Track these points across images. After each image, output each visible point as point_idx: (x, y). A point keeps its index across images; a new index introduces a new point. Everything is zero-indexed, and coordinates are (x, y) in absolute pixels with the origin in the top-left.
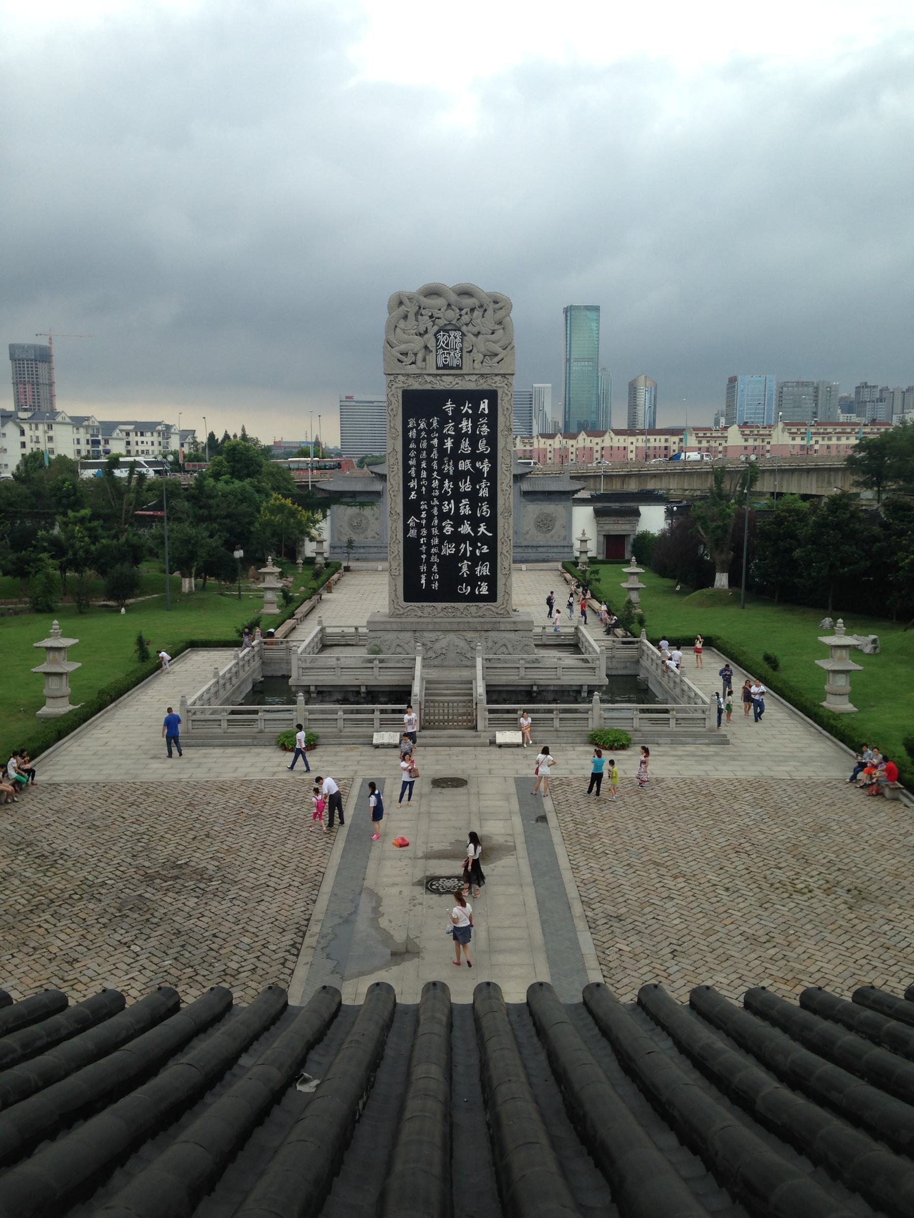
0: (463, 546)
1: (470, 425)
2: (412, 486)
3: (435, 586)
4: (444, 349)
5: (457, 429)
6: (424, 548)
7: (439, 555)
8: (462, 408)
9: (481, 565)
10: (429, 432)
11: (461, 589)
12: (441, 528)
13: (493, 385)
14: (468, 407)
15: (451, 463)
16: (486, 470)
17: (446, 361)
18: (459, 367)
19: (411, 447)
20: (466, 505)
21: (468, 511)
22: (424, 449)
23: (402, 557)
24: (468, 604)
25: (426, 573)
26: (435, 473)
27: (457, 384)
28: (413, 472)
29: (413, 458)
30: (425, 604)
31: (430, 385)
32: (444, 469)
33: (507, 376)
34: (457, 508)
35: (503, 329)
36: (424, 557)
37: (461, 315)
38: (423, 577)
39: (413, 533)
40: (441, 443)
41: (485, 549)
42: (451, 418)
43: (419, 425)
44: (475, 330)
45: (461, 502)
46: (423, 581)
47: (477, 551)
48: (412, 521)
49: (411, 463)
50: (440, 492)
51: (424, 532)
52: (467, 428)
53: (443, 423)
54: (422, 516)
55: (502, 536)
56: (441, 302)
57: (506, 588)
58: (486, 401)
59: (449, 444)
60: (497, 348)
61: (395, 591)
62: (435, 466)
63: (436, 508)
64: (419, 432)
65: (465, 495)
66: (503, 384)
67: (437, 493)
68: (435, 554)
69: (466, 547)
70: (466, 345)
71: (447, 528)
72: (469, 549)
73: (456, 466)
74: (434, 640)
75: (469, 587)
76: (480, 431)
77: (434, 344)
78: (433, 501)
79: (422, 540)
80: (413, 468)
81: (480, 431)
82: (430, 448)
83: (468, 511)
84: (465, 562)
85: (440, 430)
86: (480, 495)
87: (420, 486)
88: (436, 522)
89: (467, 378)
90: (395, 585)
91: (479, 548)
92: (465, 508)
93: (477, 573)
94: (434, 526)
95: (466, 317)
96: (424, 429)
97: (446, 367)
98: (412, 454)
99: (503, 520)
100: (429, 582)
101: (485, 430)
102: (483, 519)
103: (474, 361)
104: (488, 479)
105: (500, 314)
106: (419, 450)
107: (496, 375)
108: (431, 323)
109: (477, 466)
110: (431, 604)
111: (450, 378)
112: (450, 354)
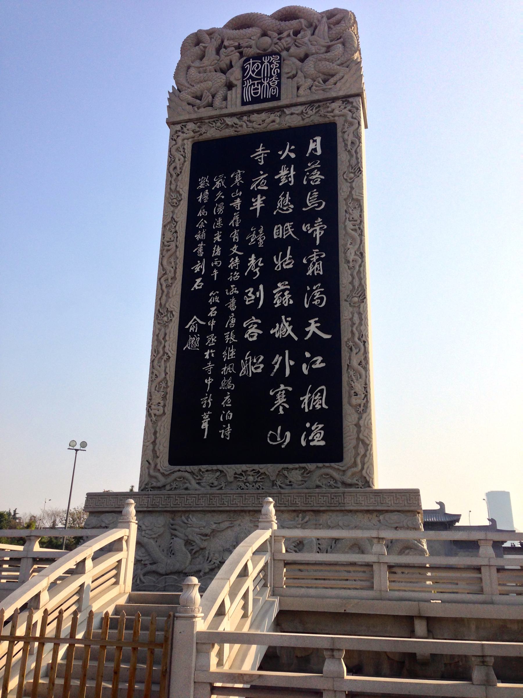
0: (278, 359)
1: (292, 173)
2: (197, 269)
3: (226, 432)
4: (253, 79)
5: (273, 183)
6: (210, 365)
7: (235, 377)
8: (280, 153)
9: (311, 392)
10: (228, 191)
11: (273, 438)
12: (240, 331)
13: (328, 114)
14: (290, 151)
15: (261, 231)
16: (318, 234)
17: (255, 93)
18: (274, 98)
19: (200, 214)
20: (284, 291)
21: (287, 300)
22: (220, 216)
23: (171, 384)
24: (285, 466)
25: (210, 410)
26: (235, 247)
27: (273, 121)
28: (200, 250)
29: (201, 230)
30: (204, 467)
31: (234, 129)
32: (249, 240)
33: (351, 100)
34: (269, 297)
35: (343, 44)
36: (209, 381)
37: (280, 39)
38: (206, 417)
39: (193, 343)
40: (247, 202)
41: (319, 363)
42: (262, 168)
43: (213, 183)
44: (301, 52)
45: (278, 287)
46: (205, 425)
47: (304, 366)
48: (191, 326)
49: (198, 237)
50: (242, 274)
51: (212, 339)
52: (287, 178)
53: (248, 179)
54: (211, 314)
55: (350, 335)
56: (255, 31)
57: (359, 432)
58: (318, 139)
59: (258, 203)
60: (335, 67)
61: (154, 443)
62: (235, 236)
63: (233, 301)
64: (213, 194)
65: (284, 275)
66: (346, 111)
67: (237, 276)
68: (228, 376)
69: (283, 361)
70: (285, 69)
71: (250, 331)
72: (289, 363)
73: (269, 233)
74: (208, 531)
75: (288, 434)
76: (309, 181)
77: (240, 76)
78: (230, 289)
79: (207, 353)
80: (201, 245)
81: (309, 181)
82: (229, 212)
83: (287, 300)
84: (282, 387)
85: (245, 187)
86: (309, 273)
87: (209, 269)
88: (233, 321)
89: (287, 111)
90: (155, 433)
91: (308, 361)
92: (283, 296)
93: (305, 406)
94: (229, 329)
95: (289, 39)
96: (221, 188)
97: (256, 100)
98: (201, 225)
99: (351, 309)
100: (215, 425)
101: (317, 177)
102: (314, 312)
103: (298, 88)
104: (321, 248)
105: (337, 29)
106: (211, 218)
107: (334, 100)
108: (238, 54)
109: (304, 229)
110: (215, 467)
111: (263, 115)
112: (262, 84)
